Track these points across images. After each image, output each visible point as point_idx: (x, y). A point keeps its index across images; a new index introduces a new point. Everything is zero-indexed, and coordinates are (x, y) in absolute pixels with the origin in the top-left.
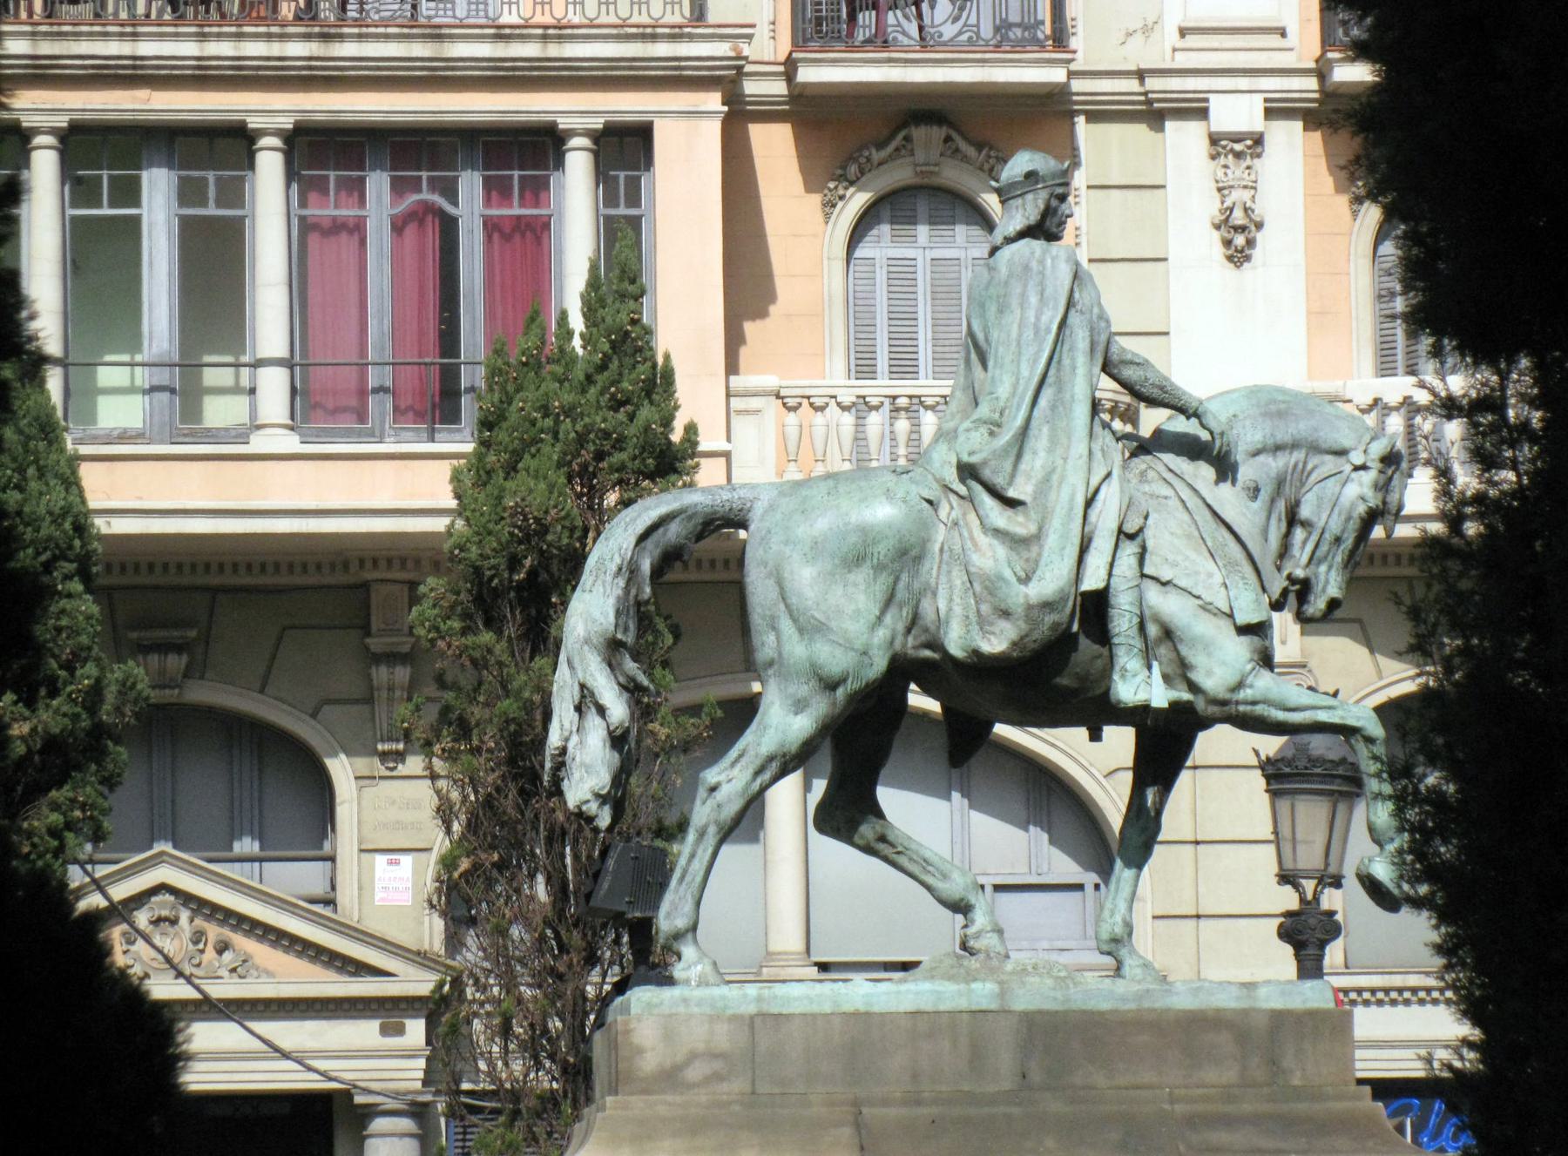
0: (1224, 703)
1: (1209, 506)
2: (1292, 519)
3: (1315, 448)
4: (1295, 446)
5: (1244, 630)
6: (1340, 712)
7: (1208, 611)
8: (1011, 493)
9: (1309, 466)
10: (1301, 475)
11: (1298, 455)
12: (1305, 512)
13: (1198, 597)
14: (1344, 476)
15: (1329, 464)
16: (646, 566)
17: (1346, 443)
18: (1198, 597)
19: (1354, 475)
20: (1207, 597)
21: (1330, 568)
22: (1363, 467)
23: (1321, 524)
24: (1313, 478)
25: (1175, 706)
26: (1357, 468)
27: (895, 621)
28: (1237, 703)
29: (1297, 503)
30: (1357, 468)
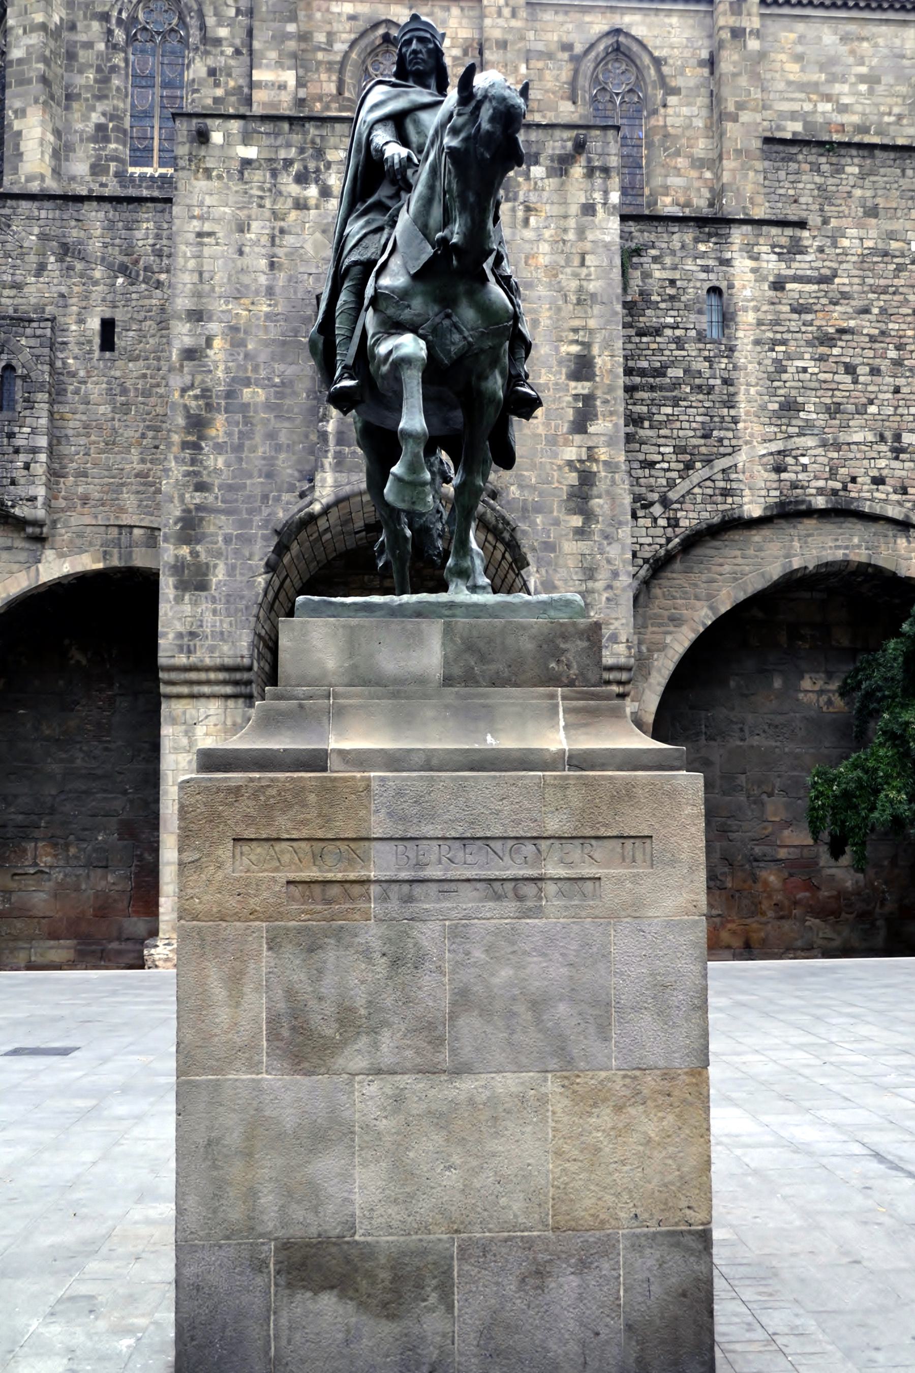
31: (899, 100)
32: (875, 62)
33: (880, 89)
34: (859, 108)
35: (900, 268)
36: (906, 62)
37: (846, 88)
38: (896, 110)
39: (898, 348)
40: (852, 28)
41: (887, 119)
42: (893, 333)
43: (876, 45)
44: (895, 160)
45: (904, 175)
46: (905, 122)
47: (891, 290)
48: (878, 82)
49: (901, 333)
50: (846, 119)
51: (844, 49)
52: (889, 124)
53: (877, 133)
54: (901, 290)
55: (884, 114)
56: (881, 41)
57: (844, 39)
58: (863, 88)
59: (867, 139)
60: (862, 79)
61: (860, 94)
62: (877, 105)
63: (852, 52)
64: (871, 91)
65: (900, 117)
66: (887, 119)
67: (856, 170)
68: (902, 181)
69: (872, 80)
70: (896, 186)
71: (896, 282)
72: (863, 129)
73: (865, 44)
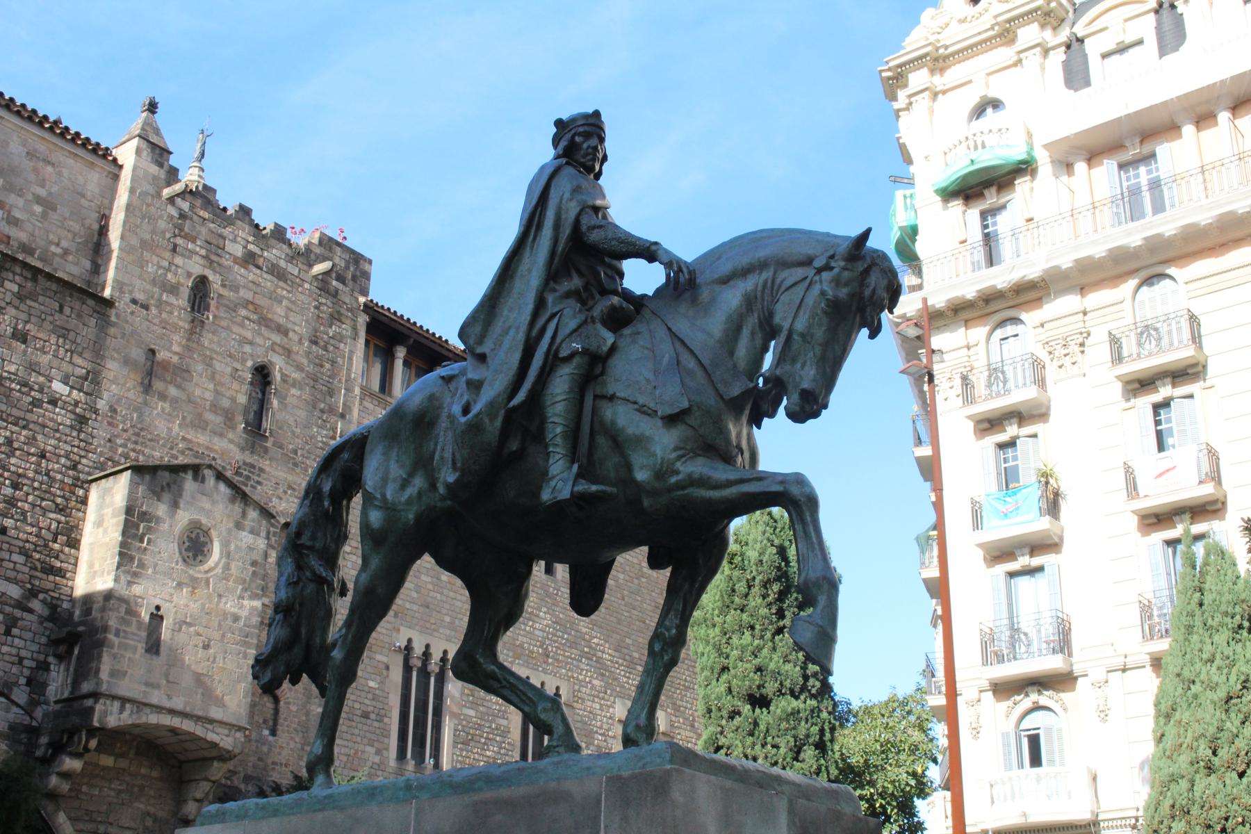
0: (654, 493)
1: (669, 329)
2: (769, 330)
3: (784, 264)
4: (762, 265)
5: (672, 420)
6: (766, 483)
7: (644, 413)
8: (479, 350)
9: (778, 281)
10: (772, 290)
11: (767, 275)
12: (777, 319)
13: (635, 403)
14: (808, 281)
15: (799, 273)
16: (327, 487)
17: (811, 252)
18: (635, 403)
19: (817, 278)
20: (641, 400)
21: (803, 366)
22: (827, 268)
23: (786, 325)
24: (783, 288)
25: (580, 500)
26: (819, 271)
27: (419, 482)
28: (671, 489)
29: (772, 314)
30: (819, 271)
31: (70, 236)
32: (55, 189)
33: (54, 216)
34: (29, 227)
35: (36, 403)
36: (83, 201)
37: (20, 202)
38: (64, 244)
39: (16, 486)
40: (42, 148)
41: (53, 248)
42: (13, 469)
43: (60, 174)
44: (56, 293)
45: (61, 310)
46: (70, 258)
47: (22, 423)
48: (54, 209)
49: (21, 471)
50: (14, 232)
51: (28, 164)
52: (54, 254)
53: (40, 259)
54: (31, 426)
55: (51, 243)
56: (65, 172)
57: (31, 155)
58: (38, 209)
59: (29, 260)
60: (39, 200)
61: (33, 213)
62: (48, 232)
63: (35, 170)
64: (44, 215)
65: (66, 252)
66: (53, 248)
67: (16, 288)
68: (57, 316)
69: (48, 205)
70: (50, 318)
71: (28, 416)
72: (25, 248)
73: (49, 169)
